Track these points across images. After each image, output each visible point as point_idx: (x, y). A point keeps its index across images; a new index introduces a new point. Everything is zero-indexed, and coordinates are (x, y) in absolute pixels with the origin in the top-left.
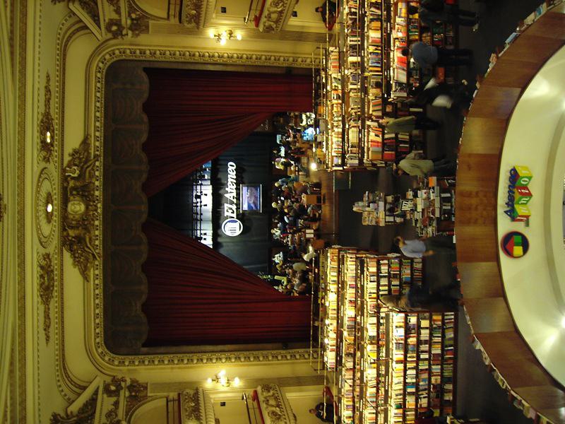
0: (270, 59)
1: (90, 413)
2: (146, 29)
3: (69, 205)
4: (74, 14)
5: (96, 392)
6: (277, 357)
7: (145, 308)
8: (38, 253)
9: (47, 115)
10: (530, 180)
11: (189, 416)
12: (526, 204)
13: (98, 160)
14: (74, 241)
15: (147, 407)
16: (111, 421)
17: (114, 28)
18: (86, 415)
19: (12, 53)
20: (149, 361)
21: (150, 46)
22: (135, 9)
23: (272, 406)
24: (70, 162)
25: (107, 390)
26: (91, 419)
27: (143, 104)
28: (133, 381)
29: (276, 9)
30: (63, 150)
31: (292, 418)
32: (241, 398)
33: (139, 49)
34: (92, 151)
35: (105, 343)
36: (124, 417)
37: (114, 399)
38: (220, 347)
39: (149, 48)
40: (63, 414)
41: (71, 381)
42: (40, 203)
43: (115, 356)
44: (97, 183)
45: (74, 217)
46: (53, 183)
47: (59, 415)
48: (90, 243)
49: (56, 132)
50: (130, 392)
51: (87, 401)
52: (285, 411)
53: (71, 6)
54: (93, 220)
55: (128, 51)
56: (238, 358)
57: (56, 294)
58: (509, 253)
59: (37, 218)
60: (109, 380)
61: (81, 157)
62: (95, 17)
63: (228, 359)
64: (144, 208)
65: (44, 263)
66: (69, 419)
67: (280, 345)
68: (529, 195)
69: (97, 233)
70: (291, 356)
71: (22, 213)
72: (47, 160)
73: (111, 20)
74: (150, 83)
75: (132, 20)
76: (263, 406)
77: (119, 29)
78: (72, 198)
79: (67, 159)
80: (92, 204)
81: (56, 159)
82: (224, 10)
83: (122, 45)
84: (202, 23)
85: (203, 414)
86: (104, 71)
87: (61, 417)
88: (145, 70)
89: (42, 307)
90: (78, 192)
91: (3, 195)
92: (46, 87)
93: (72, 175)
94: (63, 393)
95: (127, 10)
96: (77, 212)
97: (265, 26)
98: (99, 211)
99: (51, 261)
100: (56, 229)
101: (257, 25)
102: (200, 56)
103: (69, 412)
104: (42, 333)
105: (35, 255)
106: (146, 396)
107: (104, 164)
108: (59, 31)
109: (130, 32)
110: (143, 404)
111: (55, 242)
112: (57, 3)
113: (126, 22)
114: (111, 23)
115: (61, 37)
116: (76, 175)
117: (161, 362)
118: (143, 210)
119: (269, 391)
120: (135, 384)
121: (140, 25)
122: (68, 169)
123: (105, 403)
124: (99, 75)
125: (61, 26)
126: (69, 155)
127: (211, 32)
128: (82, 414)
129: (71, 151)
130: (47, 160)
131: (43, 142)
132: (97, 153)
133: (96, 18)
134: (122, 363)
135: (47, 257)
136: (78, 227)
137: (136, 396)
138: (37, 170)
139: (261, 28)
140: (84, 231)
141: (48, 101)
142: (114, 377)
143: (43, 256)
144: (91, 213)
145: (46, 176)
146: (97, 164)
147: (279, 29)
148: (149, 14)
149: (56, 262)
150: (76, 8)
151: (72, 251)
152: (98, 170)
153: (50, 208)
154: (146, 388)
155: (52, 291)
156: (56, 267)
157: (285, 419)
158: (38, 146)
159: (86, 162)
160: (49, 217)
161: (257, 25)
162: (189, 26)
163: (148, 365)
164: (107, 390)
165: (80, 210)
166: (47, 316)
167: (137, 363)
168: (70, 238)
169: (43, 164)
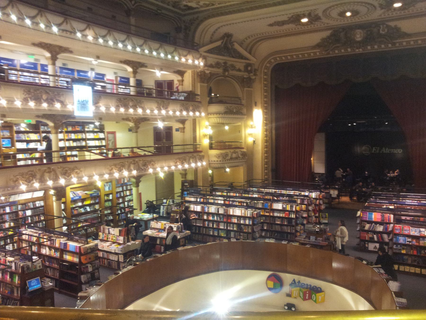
5: (246, 59)
10: (314, 301)
11: (227, 108)
12: (300, 297)
15: (237, 86)
16: (228, 67)
23: (232, 155)
25: (247, 66)
37: (242, 68)
40: (233, 40)
44: (376, 47)
50: (248, 78)
58: (269, 278)
60: (256, 67)
68: (305, 299)
69: (343, 51)
70: (266, 173)
72: (382, 7)
76: (232, 151)
78: (365, 31)
79: (392, 24)
80: (361, 45)
81: (386, 15)
85: (228, 116)
93: (381, 30)
98: (357, 50)
105: (314, 8)
116: (381, 32)
119: (242, 155)
122: (385, 26)
123: (240, 64)
126: (396, 26)
142: (257, 70)
144: (355, 45)
154: (249, 87)
157: (223, 161)
166: (283, 23)
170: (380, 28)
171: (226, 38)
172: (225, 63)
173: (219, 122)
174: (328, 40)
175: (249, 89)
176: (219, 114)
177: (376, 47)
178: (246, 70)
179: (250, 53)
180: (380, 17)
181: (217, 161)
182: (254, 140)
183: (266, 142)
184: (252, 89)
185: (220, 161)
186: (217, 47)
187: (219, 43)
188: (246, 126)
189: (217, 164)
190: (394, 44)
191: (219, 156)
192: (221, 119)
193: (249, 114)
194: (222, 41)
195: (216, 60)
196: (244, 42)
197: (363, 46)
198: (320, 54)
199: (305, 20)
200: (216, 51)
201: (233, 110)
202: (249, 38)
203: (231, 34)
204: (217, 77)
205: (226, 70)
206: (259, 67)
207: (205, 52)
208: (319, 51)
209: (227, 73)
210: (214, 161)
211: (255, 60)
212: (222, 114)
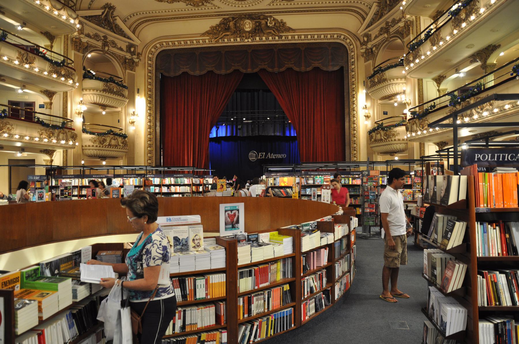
0: (355, 150)
1: (115, 31)
2: (366, 60)
3: (249, 21)
5: (129, 38)
7: (185, 73)
17: (366, 39)
18: (114, 28)
23: (110, 141)
24: (277, 20)
25: (130, 46)
29: (383, 135)
33: (355, 61)
37: (125, 49)
38: (158, 124)
40: (115, 14)
41: (138, 26)
45: (242, 25)
47: (114, 11)
48: (225, 35)
50: (130, 59)
51: (123, 31)
52: (106, 149)
53: (375, 4)
54: (240, 37)
55: (353, 54)
60: (139, 50)
61: (281, 27)
63: (150, 127)
64: (249, 71)
66: (112, 17)
69: (232, 40)
75: (371, 49)
78: (254, 23)
79: (279, 18)
81: (275, 4)
85: (107, 94)
88: (342, 68)
93: (268, 22)
96: (245, 27)
98: (246, 40)
109: (363, 51)
116: (269, 24)
118: (249, 70)
120: (134, 64)
121: (370, 54)
122: (272, 18)
123: (122, 43)
124: (335, 36)
125: (363, 3)
126: (282, 20)
129: (284, 21)
134: (150, 59)
136: (235, 28)
137: (126, 62)
142: (141, 54)
144: (244, 35)
150: (374, 8)
152: (272, 39)
154: (132, 70)
155: (191, 5)
157: (100, 147)
159: (277, 30)
162: (369, 83)
163: (148, 75)
164: (130, 46)
165: (246, 28)
168: (228, 23)
170: (268, 21)
171: (107, 9)
175: (131, 72)
176: (97, 90)
177: (264, 38)
178: (129, 50)
179: (134, 32)
181: (93, 146)
185: (97, 146)
187: (99, 12)
188: (127, 114)
189: (93, 150)
190: (280, 37)
191: (95, 141)
192: (98, 97)
193: (132, 101)
194: (103, 11)
195: (95, 32)
196: (127, 20)
197: (252, 37)
201: (113, 89)
203: (113, 6)
205: (105, 44)
206: (142, 52)
207: (82, 17)
208: (208, 39)
209: (106, 48)
210: (89, 146)
212: (100, 91)
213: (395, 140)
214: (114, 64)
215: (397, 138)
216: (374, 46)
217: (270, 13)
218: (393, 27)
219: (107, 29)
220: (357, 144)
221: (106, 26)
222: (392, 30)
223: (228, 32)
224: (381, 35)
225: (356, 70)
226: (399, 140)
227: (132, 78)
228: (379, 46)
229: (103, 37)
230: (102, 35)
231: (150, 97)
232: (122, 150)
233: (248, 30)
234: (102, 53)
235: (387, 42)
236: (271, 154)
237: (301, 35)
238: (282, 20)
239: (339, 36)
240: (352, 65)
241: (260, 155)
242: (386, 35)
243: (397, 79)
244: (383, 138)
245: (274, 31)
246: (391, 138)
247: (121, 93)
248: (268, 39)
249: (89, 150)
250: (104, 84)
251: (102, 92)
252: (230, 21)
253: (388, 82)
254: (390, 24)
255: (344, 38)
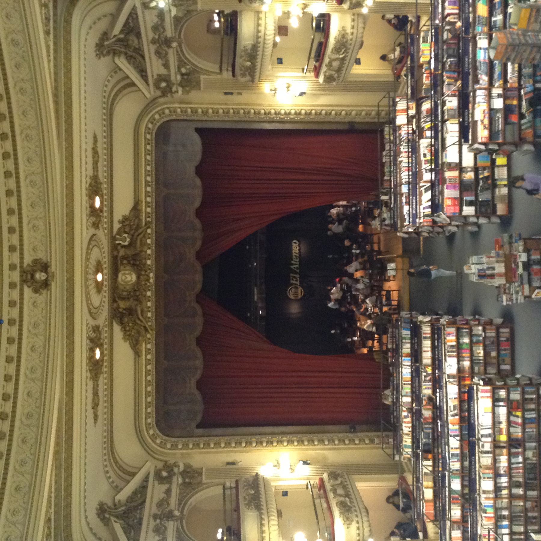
0: (330, 114)
1: (140, 502)
2: (197, 85)
3: (120, 275)
4: (120, 69)
5: (146, 479)
6: (344, 441)
7: (200, 385)
8: (87, 324)
9: (95, 178)
11: (248, 505)
13: (149, 227)
14: (125, 314)
16: (162, 511)
17: (163, 85)
19: (57, 111)
20: (204, 444)
21: (202, 104)
22: (185, 63)
23: (340, 496)
24: (119, 229)
26: (141, 509)
27: (197, 168)
28: (188, 466)
29: (338, 56)
30: (112, 217)
31: (363, 510)
32: (305, 487)
33: (191, 108)
34: (143, 218)
35: (157, 424)
36: (177, 506)
37: (165, 487)
39: (200, 106)
40: (110, 504)
41: (120, 468)
42: (90, 271)
43: (167, 438)
46: (103, 251)
47: (106, 504)
48: (142, 315)
49: (105, 197)
50: (183, 477)
51: (136, 489)
52: (355, 501)
53: (117, 61)
56: (301, 442)
57: (105, 370)
59: (87, 287)
60: (160, 465)
62: (143, 73)
63: (290, 442)
64: (199, 277)
65: (93, 335)
66: (116, 509)
67: (347, 427)
69: (149, 304)
70: (360, 440)
71: (71, 281)
73: (159, 75)
74: (203, 144)
75: (182, 75)
76: (331, 495)
77: (168, 86)
78: (122, 268)
79: (117, 226)
81: (105, 226)
82: (280, 61)
83: (173, 103)
84: (257, 77)
85: (263, 503)
86: (154, 132)
87: (108, 507)
89: (90, 384)
90: (128, 261)
91: (51, 262)
92: (93, 149)
94: (111, 480)
95: (177, 64)
96: (129, 282)
97: (325, 76)
98: (151, 281)
99: (100, 334)
100: (106, 300)
101: (317, 76)
102: (255, 113)
103: (117, 501)
104: (90, 412)
106: (200, 483)
107: (156, 232)
108: (105, 89)
109: (180, 90)
110: (197, 493)
111: (105, 313)
112: (102, 58)
113: (176, 78)
114: (160, 78)
115: (106, 95)
117: (218, 445)
118: (197, 279)
119: (336, 479)
122: (118, 237)
124: (148, 136)
126: (119, 222)
127: (266, 87)
128: (131, 503)
129: (121, 218)
130: (96, 225)
131: (92, 206)
132: (148, 219)
133: (144, 74)
134: (174, 446)
135: (96, 329)
137: (190, 483)
138: (86, 236)
139: (321, 79)
140: (136, 302)
141: (95, 163)
142: (166, 462)
143: (93, 327)
144: (143, 283)
145: (95, 243)
146: (149, 231)
147: (341, 80)
148: (201, 69)
149: (106, 335)
150: (122, 62)
151: (122, 324)
152: (149, 238)
153: (99, 277)
154: (200, 474)
156: (106, 341)
157: (356, 511)
158: (86, 211)
159: (137, 229)
160: (99, 286)
161: (317, 76)
163: (203, 448)
164: (158, 476)
166: (96, 393)
167: (191, 446)
168: (121, 310)
169: (92, 231)
170: (120, 244)
172: (155, 517)
173: (277, 523)
174: (128, 328)
175: (204, 473)
176: (262, 519)
177: (149, 252)
180: (107, 238)
181: (358, 522)
182: (302, 462)
183: (303, 442)
184: (204, 470)
185: (357, 516)
186: (125, 532)
187: (118, 527)
189: (363, 523)
191: (348, 519)
195: (151, 534)
198: (149, 343)
199: (98, 354)
200: (132, 534)
201: (251, 494)
202: (107, 472)
203: (99, 505)
204: (184, 531)
205: (170, 516)
206: (161, 460)
208: (146, 344)
209: (177, 513)
210: (358, 528)
211: (148, 464)
212: (261, 514)
213: (352, 34)
214: (194, 504)
215: (349, 30)
216: (179, 69)
217: (112, 236)
218: (164, 30)
219: (140, 514)
220: (322, 110)
221: (135, 516)
222: (169, 32)
223: (136, 311)
224: (167, 54)
225: (205, 106)
226: (353, 27)
227: (215, 472)
228: (183, 60)
229: (155, 521)
230: (152, 523)
231: (240, 443)
232: (346, 477)
233: (134, 277)
234: (184, 521)
235: (183, 46)
236: (293, 264)
237: (146, 191)
238: (119, 222)
239: (148, 131)
240: (196, 112)
241: (294, 282)
242: (174, 45)
243: (259, 25)
244: (341, 56)
245: (138, 235)
246: (347, 42)
247: (253, 483)
248: (149, 244)
249: (363, 529)
250: (248, 509)
251: (262, 511)
252: (118, 307)
253: (260, 43)
254: (157, 37)
255: (152, 123)
